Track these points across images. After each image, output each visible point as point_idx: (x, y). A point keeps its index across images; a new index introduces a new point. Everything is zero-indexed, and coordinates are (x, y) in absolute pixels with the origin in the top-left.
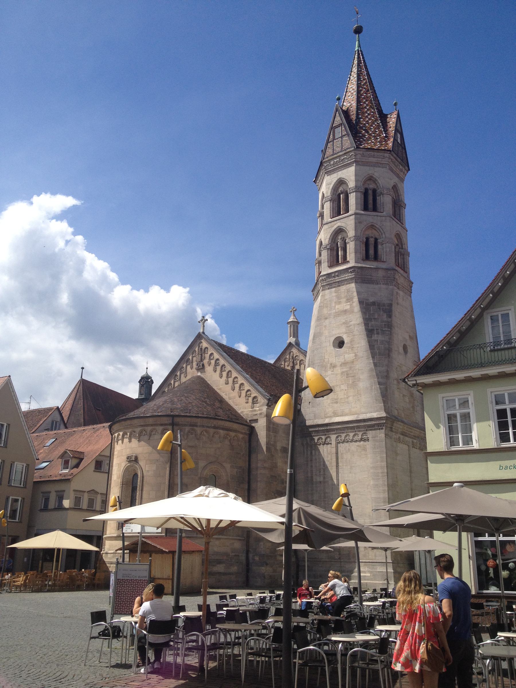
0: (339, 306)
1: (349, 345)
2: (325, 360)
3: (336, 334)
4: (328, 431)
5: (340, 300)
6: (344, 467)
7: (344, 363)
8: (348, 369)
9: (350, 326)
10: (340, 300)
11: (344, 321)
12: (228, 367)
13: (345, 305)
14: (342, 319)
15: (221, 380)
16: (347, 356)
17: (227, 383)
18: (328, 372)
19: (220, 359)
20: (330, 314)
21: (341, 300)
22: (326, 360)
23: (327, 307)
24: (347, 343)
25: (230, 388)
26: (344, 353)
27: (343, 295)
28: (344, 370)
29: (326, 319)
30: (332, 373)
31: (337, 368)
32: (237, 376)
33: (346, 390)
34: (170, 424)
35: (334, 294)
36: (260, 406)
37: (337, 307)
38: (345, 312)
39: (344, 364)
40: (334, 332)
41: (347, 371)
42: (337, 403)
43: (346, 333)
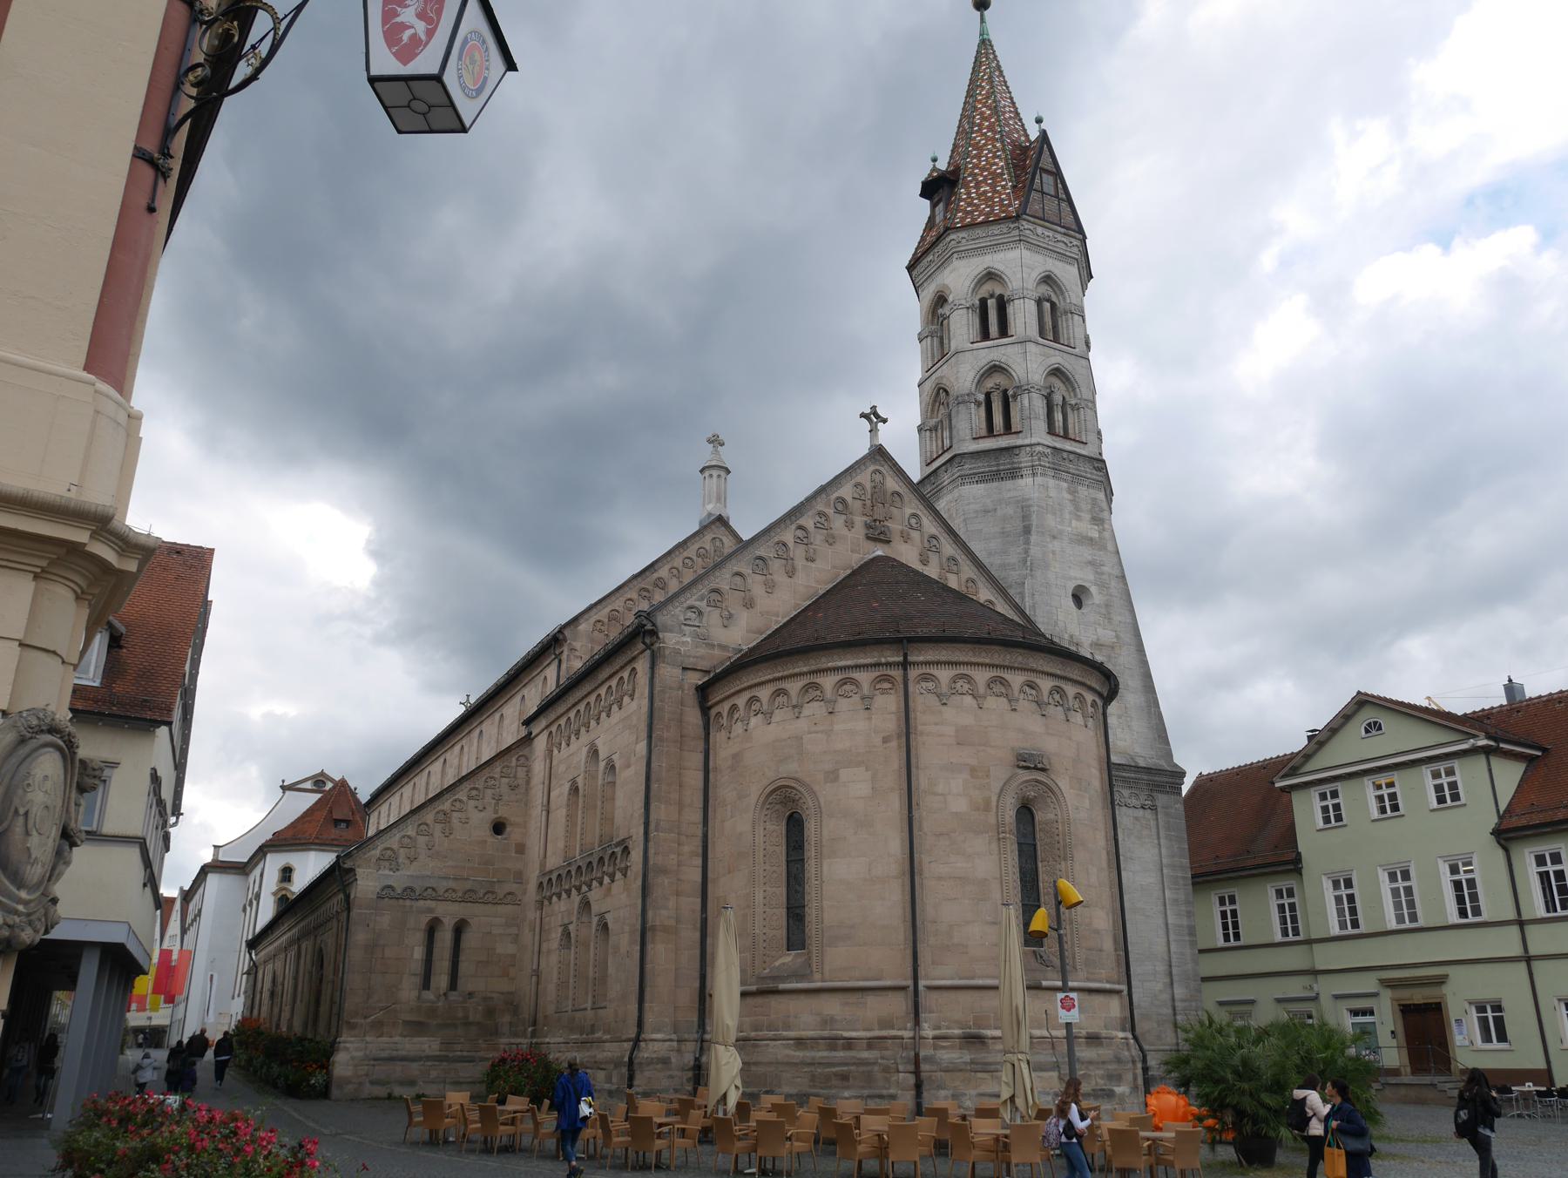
5: (1079, 513)
10: (1079, 513)
11: (1090, 558)
13: (1089, 526)
14: (1086, 553)
20: (1061, 532)
22: (1061, 624)
26: (1095, 623)
29: (1054, 537)
37: (1073, 522)
40: (1073, 573)
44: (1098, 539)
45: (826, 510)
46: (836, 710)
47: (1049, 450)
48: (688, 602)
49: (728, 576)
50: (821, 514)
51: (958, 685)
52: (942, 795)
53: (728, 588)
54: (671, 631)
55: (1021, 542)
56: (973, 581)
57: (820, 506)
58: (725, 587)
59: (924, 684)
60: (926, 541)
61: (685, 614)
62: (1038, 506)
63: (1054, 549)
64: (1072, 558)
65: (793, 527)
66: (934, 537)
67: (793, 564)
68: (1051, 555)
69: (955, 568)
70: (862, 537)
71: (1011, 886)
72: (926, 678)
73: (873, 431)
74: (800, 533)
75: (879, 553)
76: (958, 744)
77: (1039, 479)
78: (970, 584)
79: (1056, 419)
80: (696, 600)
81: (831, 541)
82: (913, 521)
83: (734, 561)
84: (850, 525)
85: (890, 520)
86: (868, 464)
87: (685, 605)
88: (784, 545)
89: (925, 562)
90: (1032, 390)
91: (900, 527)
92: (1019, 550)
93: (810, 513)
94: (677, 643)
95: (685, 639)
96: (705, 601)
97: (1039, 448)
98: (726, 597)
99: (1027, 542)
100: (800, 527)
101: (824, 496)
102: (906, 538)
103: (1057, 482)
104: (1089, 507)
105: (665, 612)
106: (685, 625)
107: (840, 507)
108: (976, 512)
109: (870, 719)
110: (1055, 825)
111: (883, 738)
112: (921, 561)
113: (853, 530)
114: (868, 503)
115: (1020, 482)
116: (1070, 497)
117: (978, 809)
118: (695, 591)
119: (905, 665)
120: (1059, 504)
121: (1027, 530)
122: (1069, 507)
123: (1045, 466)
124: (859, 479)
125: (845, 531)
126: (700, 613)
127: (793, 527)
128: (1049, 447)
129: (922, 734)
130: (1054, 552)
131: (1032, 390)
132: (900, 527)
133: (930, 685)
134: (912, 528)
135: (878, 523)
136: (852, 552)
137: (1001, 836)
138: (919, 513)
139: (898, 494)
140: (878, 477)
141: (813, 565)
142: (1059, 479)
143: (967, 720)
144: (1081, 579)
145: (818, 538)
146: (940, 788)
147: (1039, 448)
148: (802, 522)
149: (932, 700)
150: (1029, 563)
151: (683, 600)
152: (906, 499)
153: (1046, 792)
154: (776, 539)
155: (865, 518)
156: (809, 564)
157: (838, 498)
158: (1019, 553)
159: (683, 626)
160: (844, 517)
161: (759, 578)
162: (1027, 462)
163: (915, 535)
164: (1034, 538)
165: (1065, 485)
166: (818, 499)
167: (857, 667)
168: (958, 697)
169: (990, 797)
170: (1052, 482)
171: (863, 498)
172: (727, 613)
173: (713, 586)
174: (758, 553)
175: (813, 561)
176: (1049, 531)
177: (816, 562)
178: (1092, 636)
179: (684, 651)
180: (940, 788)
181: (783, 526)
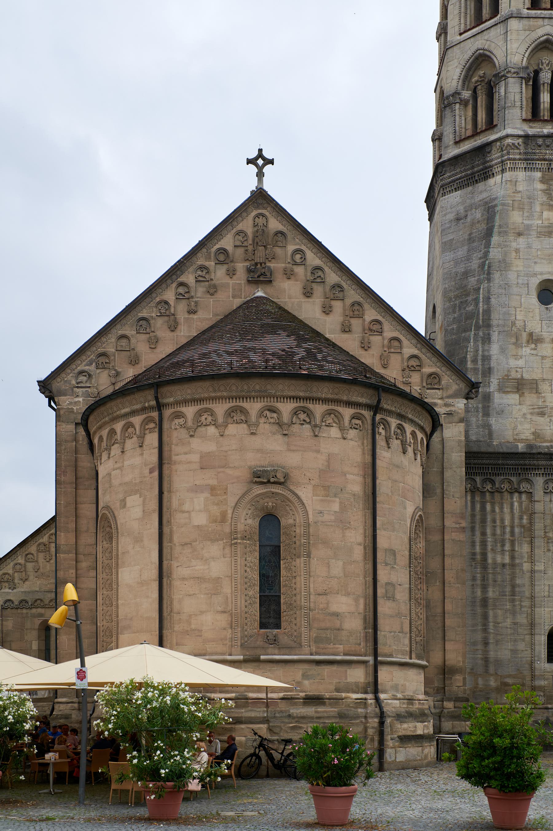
2: (517, 322)
4: (527, 469)
12: (352, 292)
15: (329, 319)
17: (346, 329)
18: (524, 349)
19: (326, 269)
20: (528, 228)
23: (522, 209)
25: (357, 344)
29: (520, 234)
30: (533, 352)
32: (380, 318)
34: (368, 407)
35: (540, 186)
36: (448, 397)
45: (207, 264)
46: (125, 450)
47: (520, 140)
48: (79, 368)
49: (113, 340)
50: (202, 268)
51: (203, 418)
52: (187, 512)
53: (114, 350)
54: (65, 395)
55: (483, 247)
56: (359, 304)
57: (200, 261)
58: (111, 349)
59: (177, 421)
60: (309, 274)
61: (77, 377)
62: (503, 205)
63: (518, 247)
64: (539, 253)
65: (174, 285)
66: (318, 268)
67: (176, 318)
68: (514, 254)
69: (340, 295)
70: (243, 282)
71: (239, 581)
72: (179, 415)
73: (260, 175)
74: (181, 290)
75: (260, 294)
76: (201, 468)
77: (508, 175)
78: (356, 307)
79: (542, 100)
80: (85, 366)
81: (212, 291)
82: (298, 257)
83: (118, 326)
84: (231, 273)
85: (273, 260)
86: (249, 210)
87: (76, 371)
88: (166, 303)
89: (308, 293)
90: (509, 75)
91: (283, 265)
92: (480, 255)
93: (191, 269)
94: (71, 403)
95: (77, 399)
96: (94, 364)
97: (509, 141)
98: (112, 358)
99: (488, 245)
100: (182, 284)
101: (204, 250)
102: (289, 275)
103: (528, 173)
105: (59, 380)
106: (78, 387)
107: (222, 258)
108: (451, 221)
109: (142, 454)
110: (293, 529)
111: (150, 469)
112: (305, 294)
113: (235, 277)
114: (250, 248)
115: (491, 181)
117: (215, 521)
118: (84, 357)
119: (160, 407)
120: (529, 198)
121: (489, 233)
123: (514, 159)
124: (240, 227)
125: (227, 280)
126: (90, 376)
127: (174, 285)
128: (519, 136)
129: (175, 463)
130: (517, 251)
131: (509, 75)
132: (283, 265)
133: (181, 421)
134: (296, 264)
135: (259, 266)
136: (233, 297)
137: (233, 542)
138: (303, 248)
139: (282, 233)
140: (261, 221)
141: (195, 317)
142: (531, 169)
143: (211, 447)
145: (199, 292)
146: (186, 507)
147: (509, 141)
148: (182, 279)
149: (183, 434)
150: (486, 267)
151: (74, 367)
152: (289, 236)
153: (284, 501)
154: (158, 299)
155: (247, 264)
156: (191, 316)
157: (219, 249)
158: (480, 258)
159: (75, 389)
160: (225, 267)
161: (144, 337)
162: (498, 158)
163: (299, 270)
164: (495, 239)
165: (538, 175)
166: (199, 255)
167: (133, 413)
168: (202, 429)
169: (227, 511)
170: (521, 175)
171: (245, 244)
172: (114, 372)
173: (100, 350)
174: (140, 315)
175: (195, 312)
176: (515, 228)
177: (198, 313)
179: (77, 409)
180: (186, 507)
181: (164, 286)
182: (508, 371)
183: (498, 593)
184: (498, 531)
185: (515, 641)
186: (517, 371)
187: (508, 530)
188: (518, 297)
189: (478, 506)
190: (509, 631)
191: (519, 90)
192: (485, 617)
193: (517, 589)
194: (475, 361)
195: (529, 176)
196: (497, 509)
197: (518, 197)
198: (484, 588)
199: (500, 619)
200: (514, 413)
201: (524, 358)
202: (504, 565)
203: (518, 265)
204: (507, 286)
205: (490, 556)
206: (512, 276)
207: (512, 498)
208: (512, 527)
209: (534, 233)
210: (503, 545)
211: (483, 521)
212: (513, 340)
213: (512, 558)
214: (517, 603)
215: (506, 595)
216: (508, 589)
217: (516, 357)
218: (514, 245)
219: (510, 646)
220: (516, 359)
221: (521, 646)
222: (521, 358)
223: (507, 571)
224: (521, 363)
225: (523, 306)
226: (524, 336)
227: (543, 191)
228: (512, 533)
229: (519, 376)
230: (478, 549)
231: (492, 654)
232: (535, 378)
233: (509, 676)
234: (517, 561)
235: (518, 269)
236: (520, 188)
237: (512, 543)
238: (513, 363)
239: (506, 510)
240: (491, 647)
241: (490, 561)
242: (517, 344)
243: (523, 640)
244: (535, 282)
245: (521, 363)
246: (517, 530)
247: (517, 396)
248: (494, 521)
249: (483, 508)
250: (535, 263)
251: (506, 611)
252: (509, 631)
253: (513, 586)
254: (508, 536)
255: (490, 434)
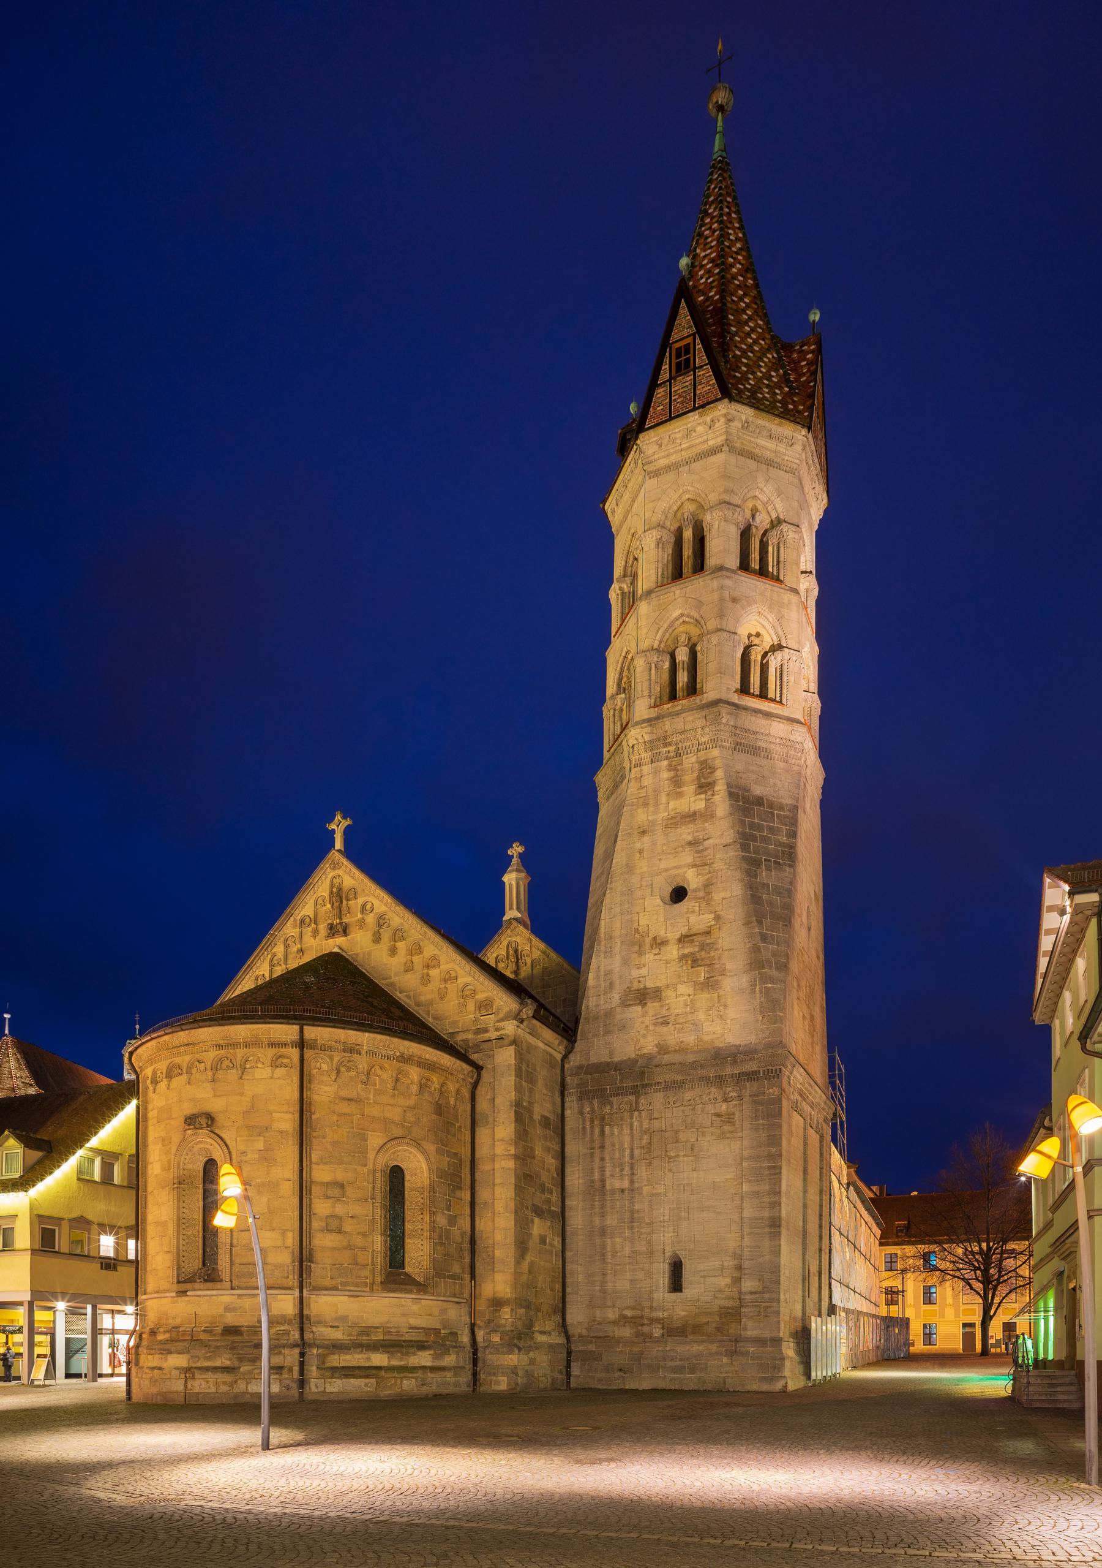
0: (678, 802)
1: (701, 894)
3: (667, 870)
5: (679, 790)
6: (681, 1159)
7: (687, 936)
8: (697, 949)
9: (703, 850)
10: (679, 790)
11: (690, 838)
14: (686, 833)
16: (693, 919)
18: (647, 956)
20: (652, 824)
21: (684, 789)
23: (646, 805)
24: (695, 891)
26: (688, 912)
27: (688, 778)
28: (687, 951)
29: (643, 833)
30: (656, 957)
31: (668, 948)
33: (689, 995)
35: (665, 775)
37: (672, 804)
38: (692, 817)
39: (684, 939)
41: (693, 954)
42: (666, 1023)
43: (694, 866)
44: (703, 811)
68: (638, 855)
104: (696, 774)
116: (672, 774)
122: (667, 786)
130: (641, 851)
144: (675, 867)
178: (682, 929)
182: (631, 982)
183: (616, 1221)
184: (617, 1155)
185: (634, 1270)
186: (639, 981)
187: (627, 1152)
188: (641, 901)
189: (597, 1131)
190: (627, 1260)
191: (648, 678)
192: (604, 1246)
193: (636, 1215)
194: (597, 978)
195: (655, 768)
196: (616, 1132)
197: (643, 793)
198: (603, 1215)
199: (618, 1248)
200: (637, 1025)
201: (647, 967)
202: (623, 1191)
203: (643, 866)
204: (631, 891)
205: (608, 1182)
206: (635, 880)
207: (632, 1118)
208: (632, 1150)
209: (659, 829)
210: (622, 1170)
211: (602, 1147)
212: (637, 948)
213: (632, 1182)
214: (636, 1230)
215: (624, 1222)
216: (627, 1216)
217: (639, 966)
218: (638, 845)
219: (628, 1275)
220: (638, 968)
221: (640, 1275)
222: (644, 966)
223: (626, 1196)
224: (644, 971)
225: (647, 910)
226: (648, 940)
227: (670, 779)
228: (632, 1156)
229: (642, 986)
230: (597, 1176)
231: (609, 1286)
232: (659, 984)
233: (627, 1308)
234: (636, 1185)
235: (643, 870)
236: (645, 782)
237: (632, 1167)
238: (635, 973)
239: (626, 1131)
240: (609, 1277)
241: (608, 1187)
242: (640, 954)
243: (642, 1269)
244: (660, 880)
245: (644, 971)
246: (637, 1152)
247: (639, 1008)
248: (613, 1145)
249: (602, 1132)
250: (660, 859)
251: (625, 1239)
252: (627, 1260)
253: (632, 1212)
254: (627, 1159)
255: (611, 1053)
